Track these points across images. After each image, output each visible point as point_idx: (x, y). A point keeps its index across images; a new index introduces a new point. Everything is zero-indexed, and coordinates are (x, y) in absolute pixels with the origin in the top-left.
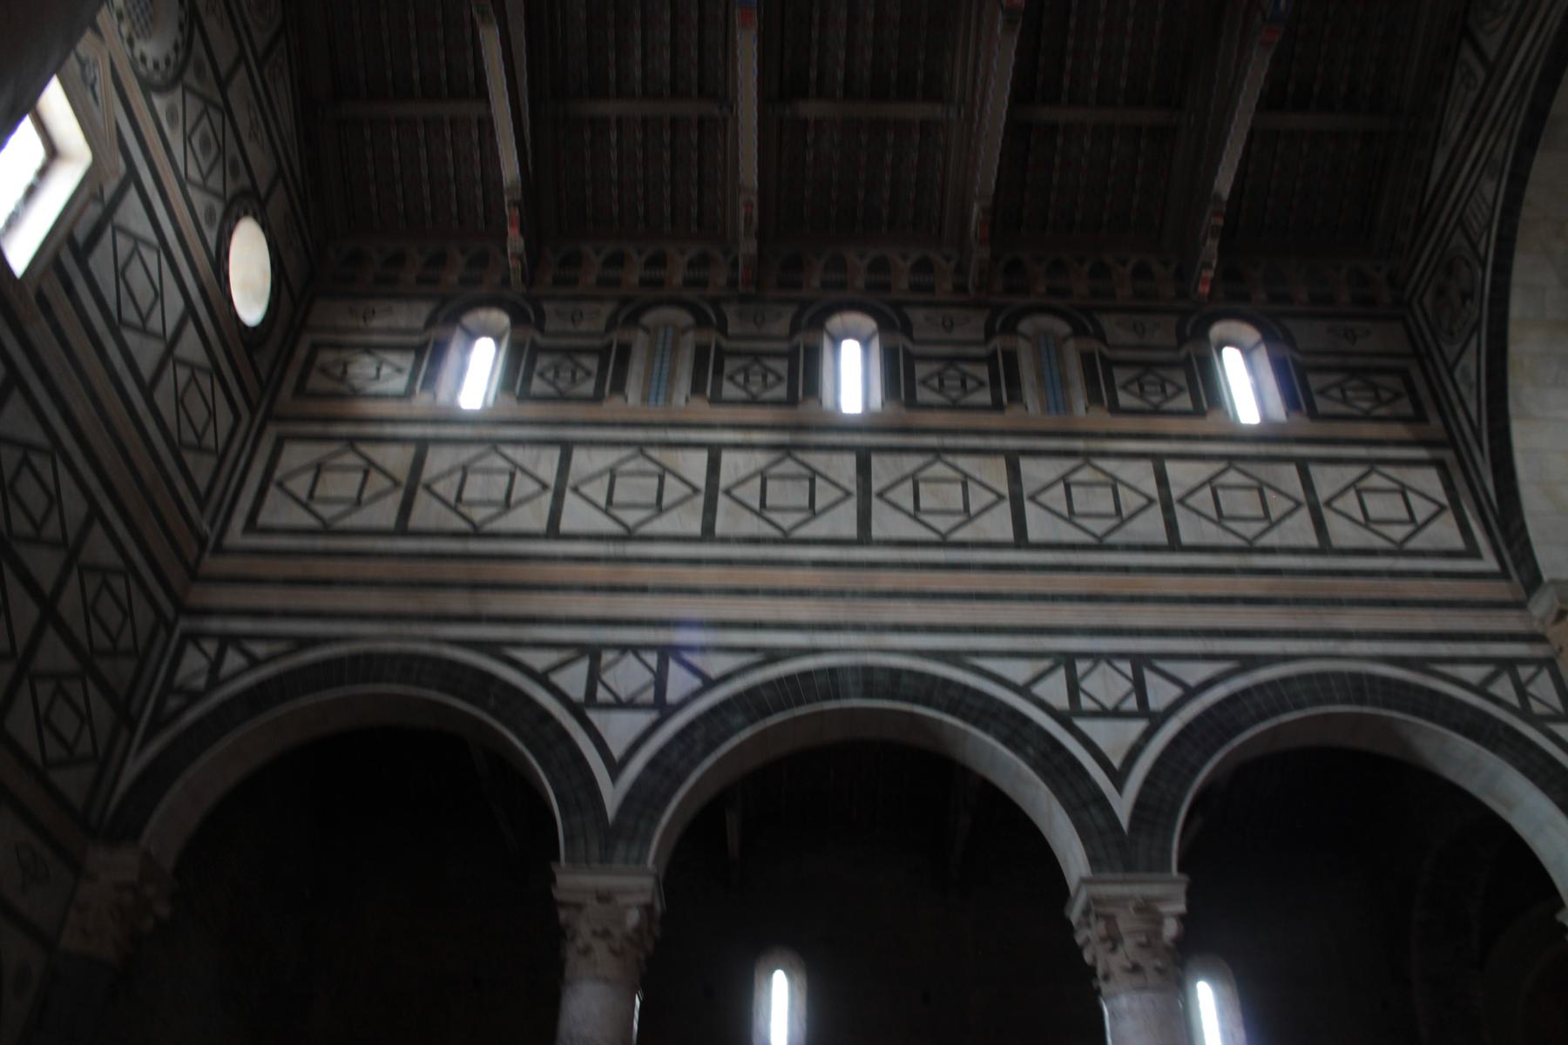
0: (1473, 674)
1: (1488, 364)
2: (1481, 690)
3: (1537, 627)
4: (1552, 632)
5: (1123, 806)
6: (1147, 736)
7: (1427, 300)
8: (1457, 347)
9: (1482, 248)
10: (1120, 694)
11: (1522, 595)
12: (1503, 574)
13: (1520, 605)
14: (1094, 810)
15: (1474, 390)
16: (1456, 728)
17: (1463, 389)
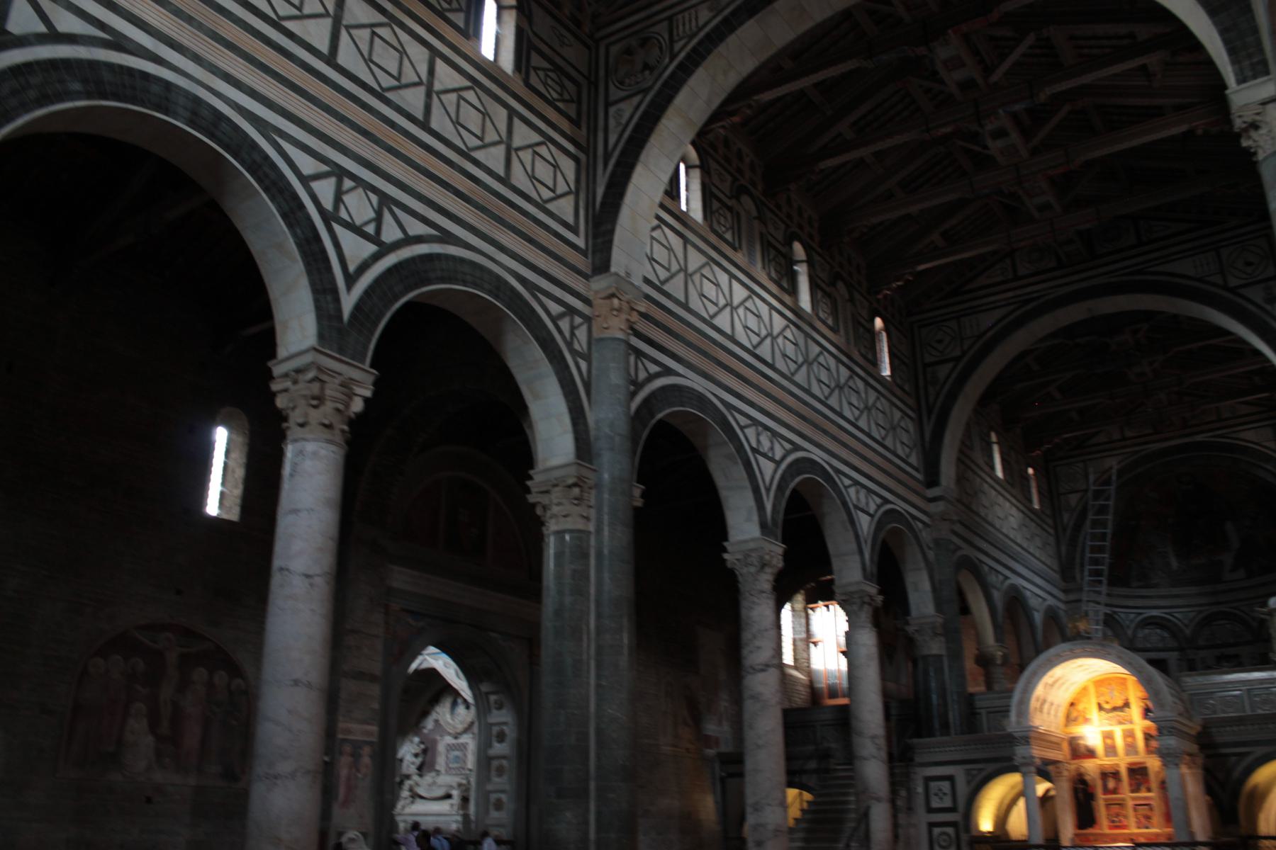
0: (555, 309)
1: (641, 118)
2: (554, 320)
3: (591, 296)
4: (597, 302)
5: (348, 302)
6: (376, 257)
7: (614, 50)
8: (623, 94)
9: (677, 47)
10: (366, 218)
11: (589, 272)
12: (584, 253)
13: (586, 277)
14: (329, 298)
15: (620, 128)
16: (537, 339)
17: (612, 122)
